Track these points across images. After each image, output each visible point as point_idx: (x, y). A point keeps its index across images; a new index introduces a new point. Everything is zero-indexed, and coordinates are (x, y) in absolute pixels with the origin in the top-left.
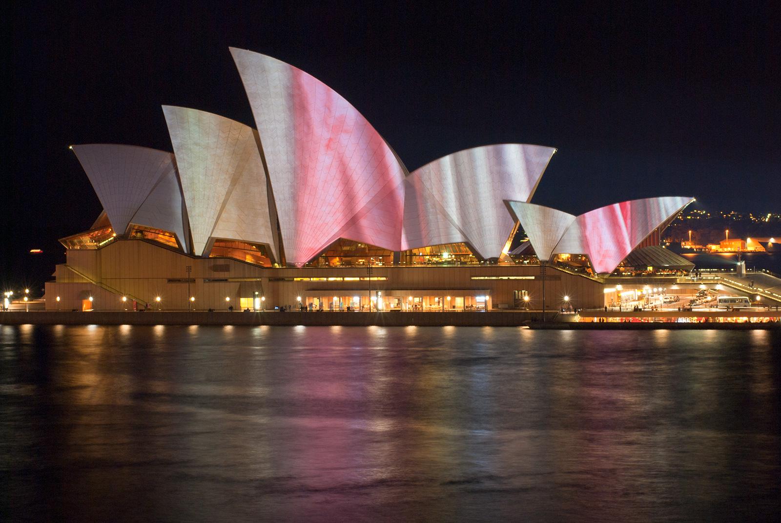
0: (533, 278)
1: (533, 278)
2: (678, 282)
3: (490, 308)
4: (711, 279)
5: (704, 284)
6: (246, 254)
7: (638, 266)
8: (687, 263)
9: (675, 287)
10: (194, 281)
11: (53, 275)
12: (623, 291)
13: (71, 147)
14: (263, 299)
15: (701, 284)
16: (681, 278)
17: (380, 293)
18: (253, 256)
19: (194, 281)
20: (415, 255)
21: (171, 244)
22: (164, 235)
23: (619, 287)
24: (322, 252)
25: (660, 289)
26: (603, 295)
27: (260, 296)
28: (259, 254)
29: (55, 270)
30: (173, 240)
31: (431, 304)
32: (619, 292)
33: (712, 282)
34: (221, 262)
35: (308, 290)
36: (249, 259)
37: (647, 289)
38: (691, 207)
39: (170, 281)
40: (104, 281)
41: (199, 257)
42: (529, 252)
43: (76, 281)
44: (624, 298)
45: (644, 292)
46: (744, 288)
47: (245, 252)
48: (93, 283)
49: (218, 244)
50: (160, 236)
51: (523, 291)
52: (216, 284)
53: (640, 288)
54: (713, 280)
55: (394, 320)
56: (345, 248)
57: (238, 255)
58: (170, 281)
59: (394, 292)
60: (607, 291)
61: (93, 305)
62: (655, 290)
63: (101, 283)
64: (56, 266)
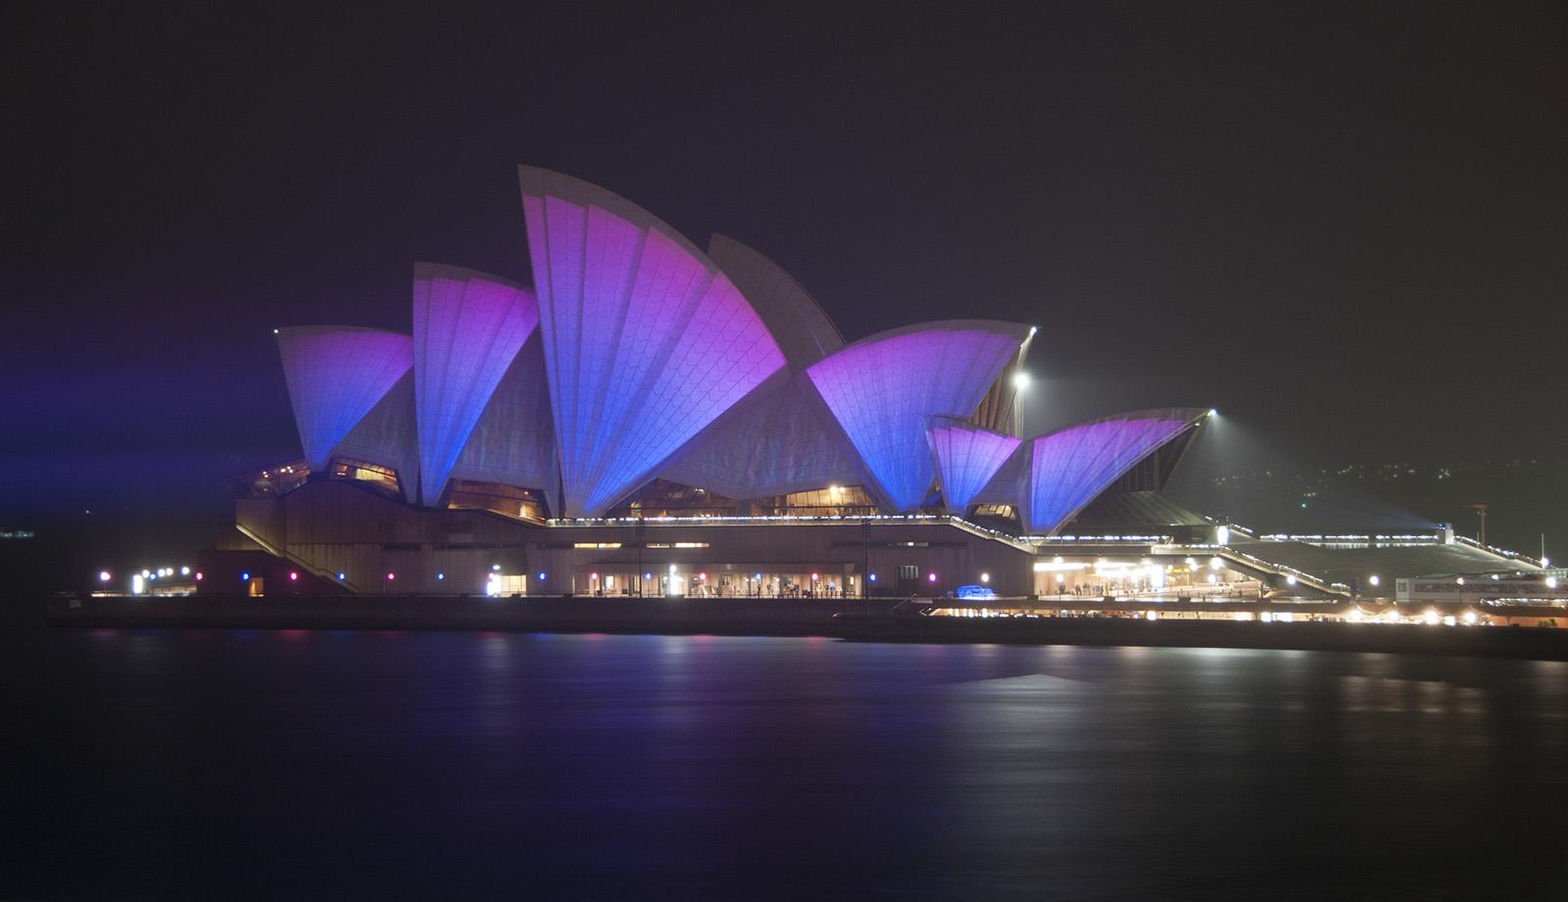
2: (1153, 552)
3: (858, 591)
4: (1205, 549)
5: (1192, 556)
10: (417, 547)
19: (417, 547)
31: (768, 586)
33: (1206, 553)
35: (593, 563)
40: (289, 548)
41: (428, 508)
43: (245, 548)
46: (1257, 563)
47: (518, 502)
48: (272, 551)
51: (912, 567)
52: (454, 553)
60: (1039, 567)
63: (286, 551)
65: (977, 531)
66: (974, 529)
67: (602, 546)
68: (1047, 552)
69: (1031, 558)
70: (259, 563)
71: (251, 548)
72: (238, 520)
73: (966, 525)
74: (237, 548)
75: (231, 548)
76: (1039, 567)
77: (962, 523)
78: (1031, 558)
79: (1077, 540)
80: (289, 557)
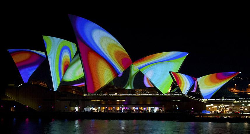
0: (180, 101)
1: (180, 101)
5: (244, 104)
6: (74, 90)
7: (218, 96)
8: (238, 96)
9: (233, 105)
12: (213, 106)
14: (79, 107)
15: (242, 104)
16: (235, 102)
17: (123, 106)
18: (75, 91)
20: (136, 91)
21: (45, 86)
22: (42, 83)
23: (212, 105)
24: (101, 90)
25: (227, 106)
27: (78, 106)
28: (78, 90)
30: (46, 85)
32: (212, 106)
33: (247, 103)
35: (96, 104)
36: (74, 92)
37: (222, 106)
38: (239, 75)
41: (55, 91)
42: (179, 91)
43: (9, 100)
44: (213, 108)
45: (221, 107)
50: (41, 83)
53: (219, 106)
54: (248, 102)
55: (128, 116)
56: (111, 89)
57: (70, 91)
59: (128, 105)
60: (207, 106)
61: (15, 109)
62: (225, 106)
65: (193, 98)
66: (192, 97)
67: (95, 100)
68: (209, 103)
69: (205, 104)
70: (13, 103)
71: (11, 100)
73: (190, 97)
75: (5, 100)
77: (188, 96)
78: (205, 104)
79: (216, 100)
80: (20, 102)
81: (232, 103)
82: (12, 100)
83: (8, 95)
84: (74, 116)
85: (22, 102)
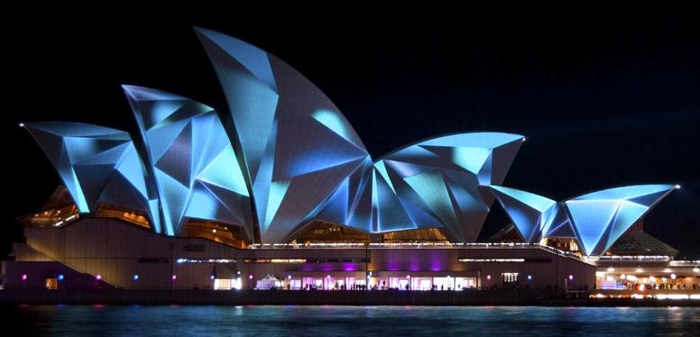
0: (523, 260)
1: (523, 260)
7: (628, 246)
11: (11, 255)
13: (22, 125)
15: (694, 267)
26: (595, 277)
29: (10, 250)
34: (195, 242)
39: (141, 260)
40: (67, 261)
43: (38, 259)
49: (189, 224)
58: (141, 260)
60: (599, 274)
64: (15, 246)
68: (603, 265)
70: (52, 269)
71: (43, 260)
72: (28, 242)
74: (32, 260)
75: (28, 260)
76: (599, 274)
78: (591, 269)
81: (664, 265)
82: (48, 260)
83: (35, 246)
84: (228, 298)
85: (81, 267)
